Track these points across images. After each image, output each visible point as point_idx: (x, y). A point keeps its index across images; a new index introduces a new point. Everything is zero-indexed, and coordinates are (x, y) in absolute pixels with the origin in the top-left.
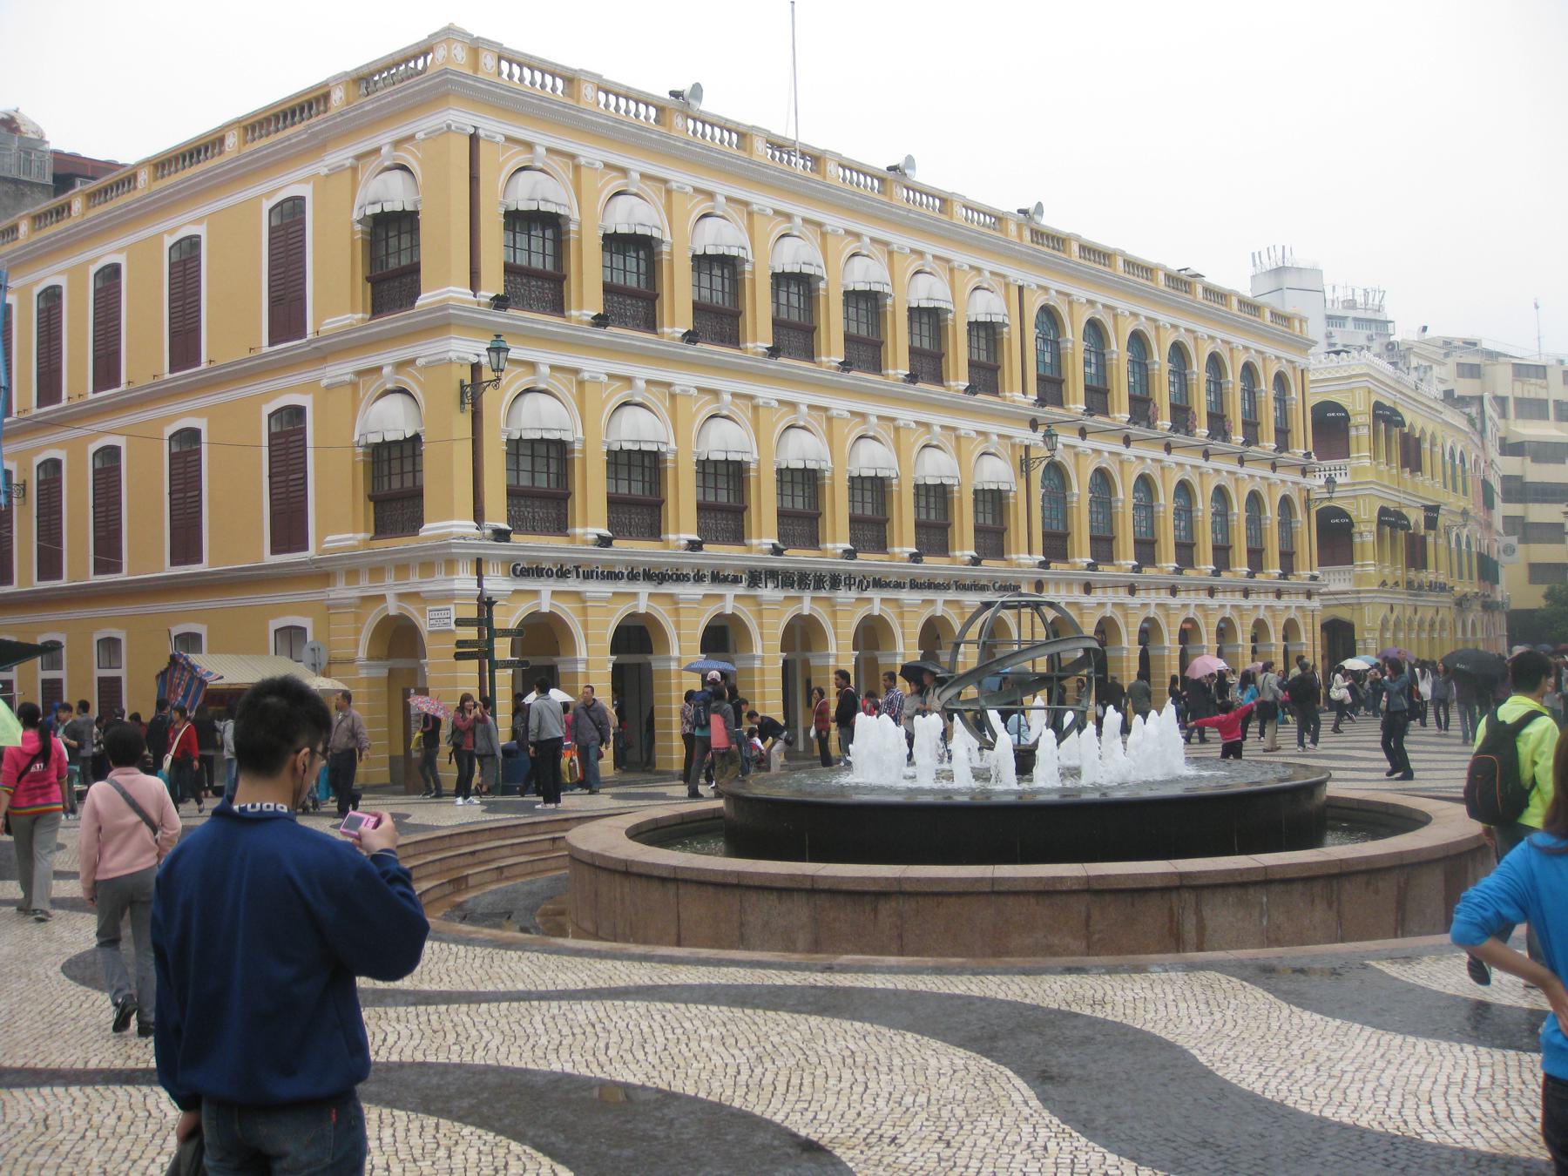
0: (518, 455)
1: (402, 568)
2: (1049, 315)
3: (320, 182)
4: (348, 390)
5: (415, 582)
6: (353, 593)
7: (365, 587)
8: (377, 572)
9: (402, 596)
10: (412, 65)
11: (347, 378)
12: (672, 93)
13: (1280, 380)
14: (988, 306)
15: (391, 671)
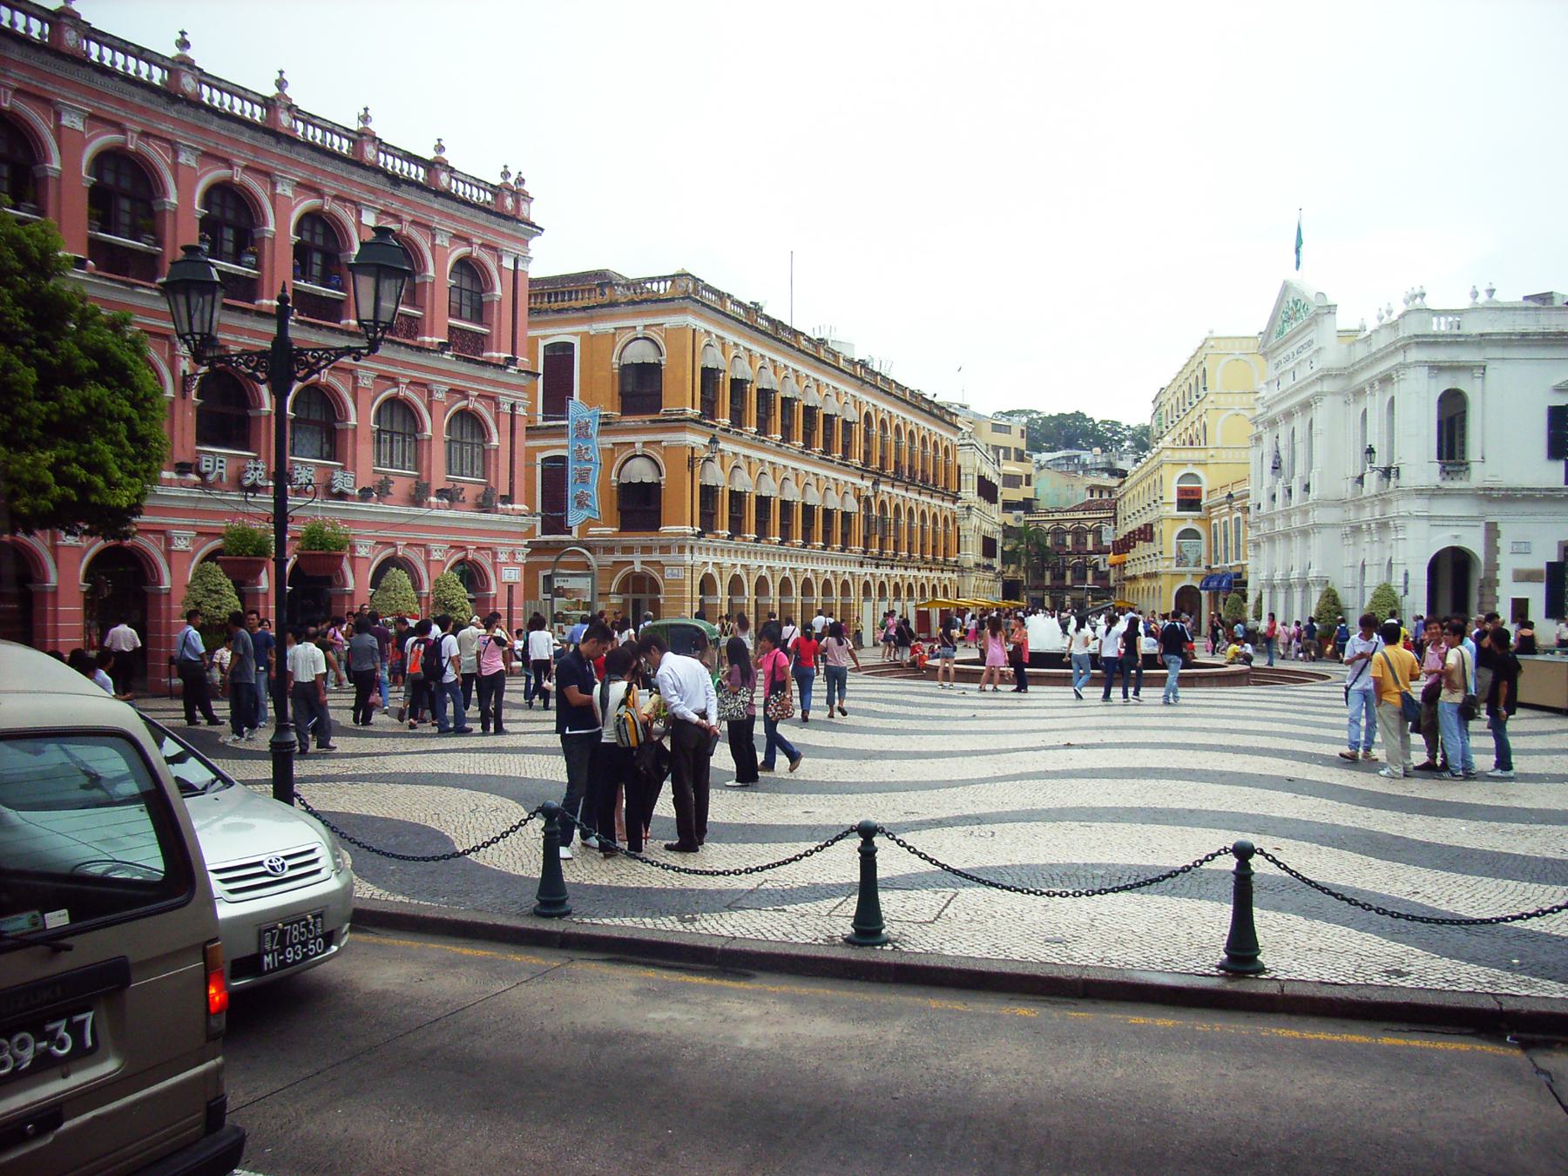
0: (379, 442)
1: (647, 549)
2: (868, 416)
3: (587, 338)
4: (609, 453)
5: (656, 556)
6: (609, 559)
7: (618, 556)
8: (628, 549)
9: (643, 563)
10: (648, 285)
11: (611, 446)
12: (751, 303)
13: (946, 448)
14: (852, 415)
15: (624, 600)
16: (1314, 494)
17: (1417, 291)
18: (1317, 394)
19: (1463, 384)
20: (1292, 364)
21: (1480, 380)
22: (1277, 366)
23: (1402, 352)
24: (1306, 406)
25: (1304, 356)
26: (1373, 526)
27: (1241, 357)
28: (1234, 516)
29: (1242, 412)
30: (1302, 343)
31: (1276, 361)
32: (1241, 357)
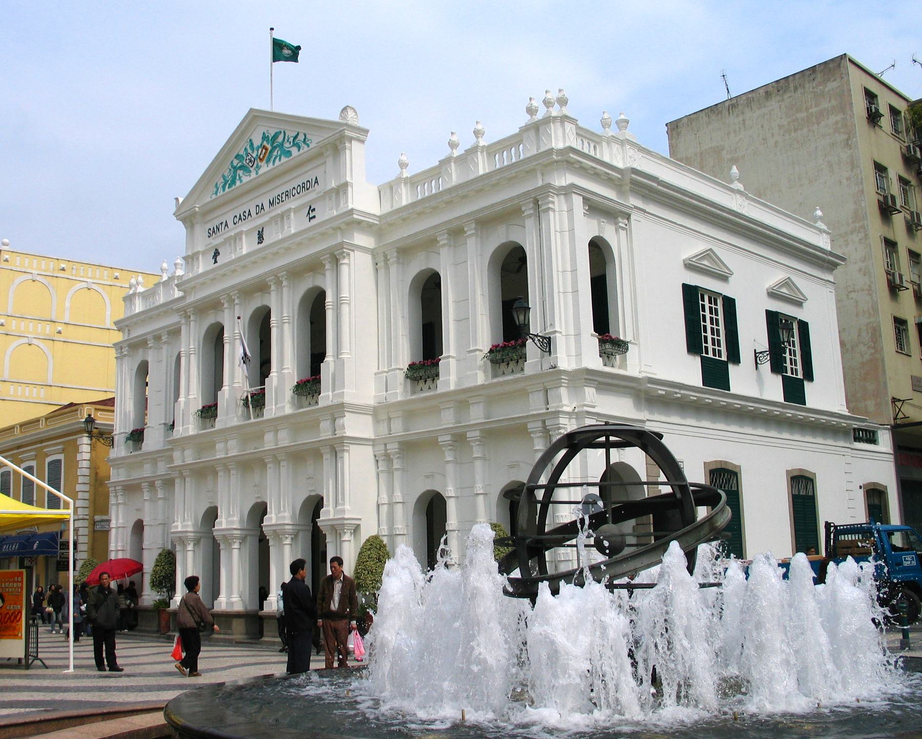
16: (327, 396)
17: (553, 95)
18: (341, 246)
19: (610, 234)
20: (266, 219)
21: (622, 233)
22: (213, 232)
23: (539, 175)
24: (313, 266)
25: (292, 204)
26: (473, 434)
27: (38, 278)
28: (48, 460)
29: (35, 342)
30: (288, 187)
31: (211, 225)
32: (38, 278)
